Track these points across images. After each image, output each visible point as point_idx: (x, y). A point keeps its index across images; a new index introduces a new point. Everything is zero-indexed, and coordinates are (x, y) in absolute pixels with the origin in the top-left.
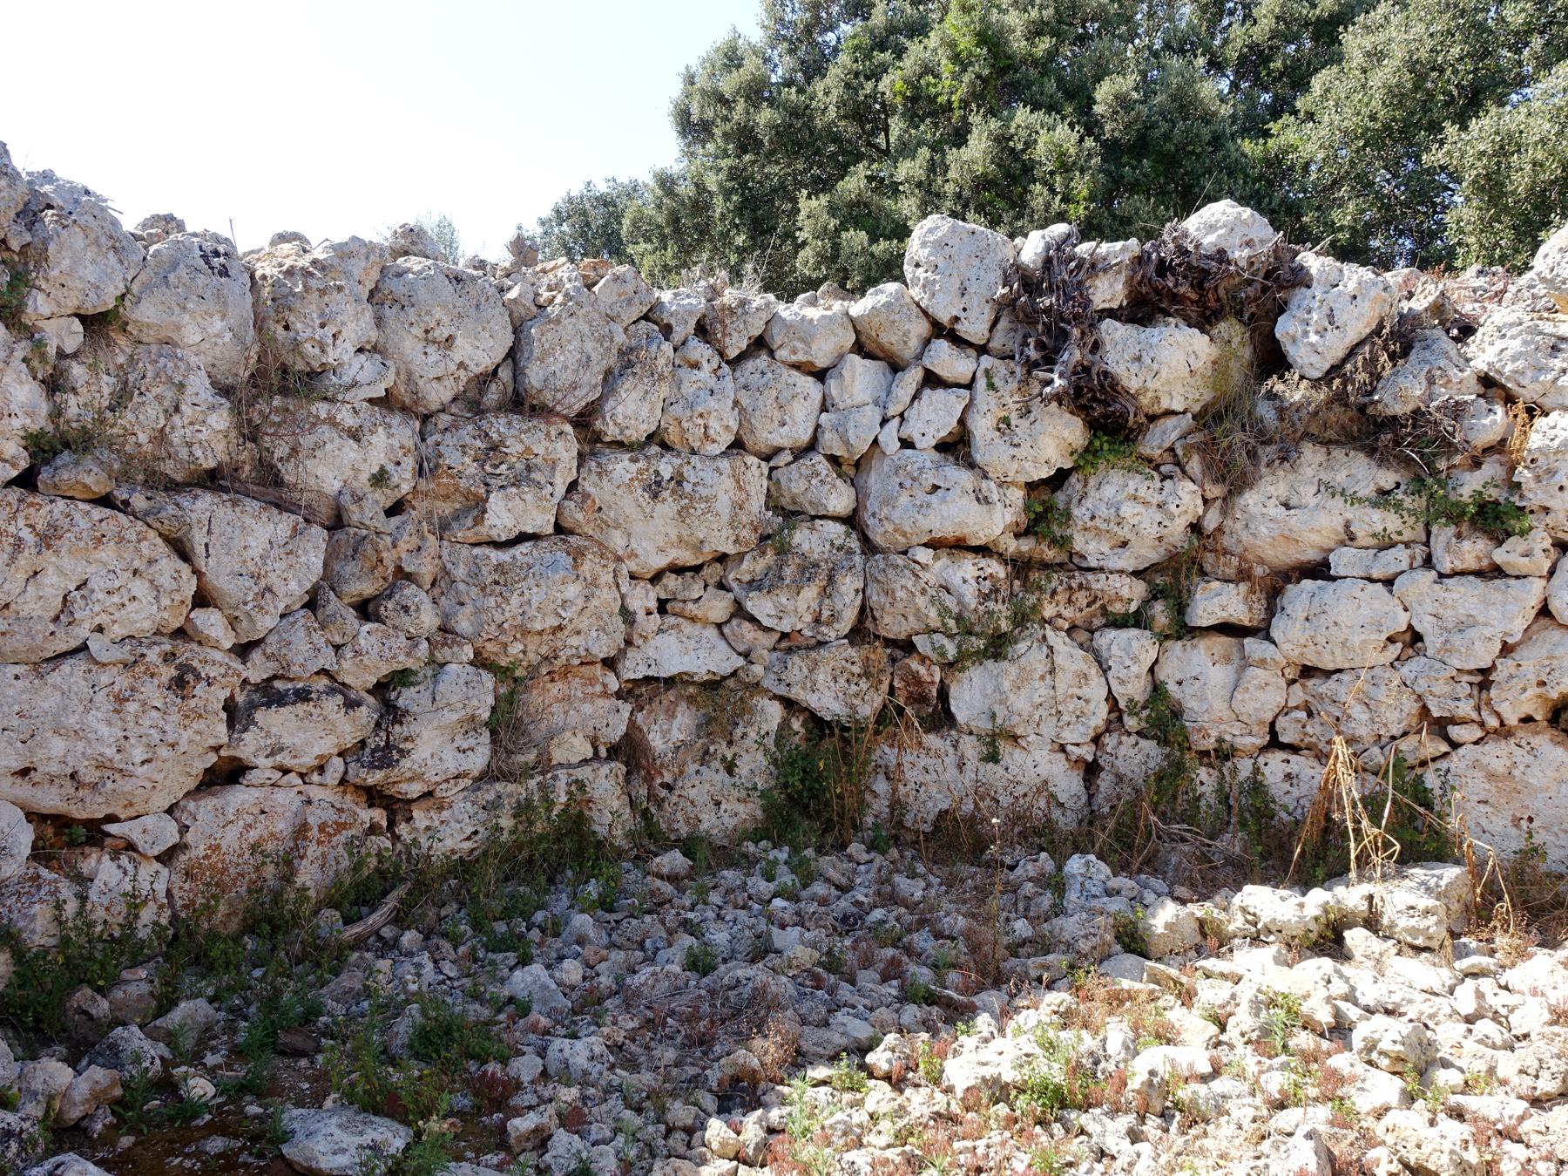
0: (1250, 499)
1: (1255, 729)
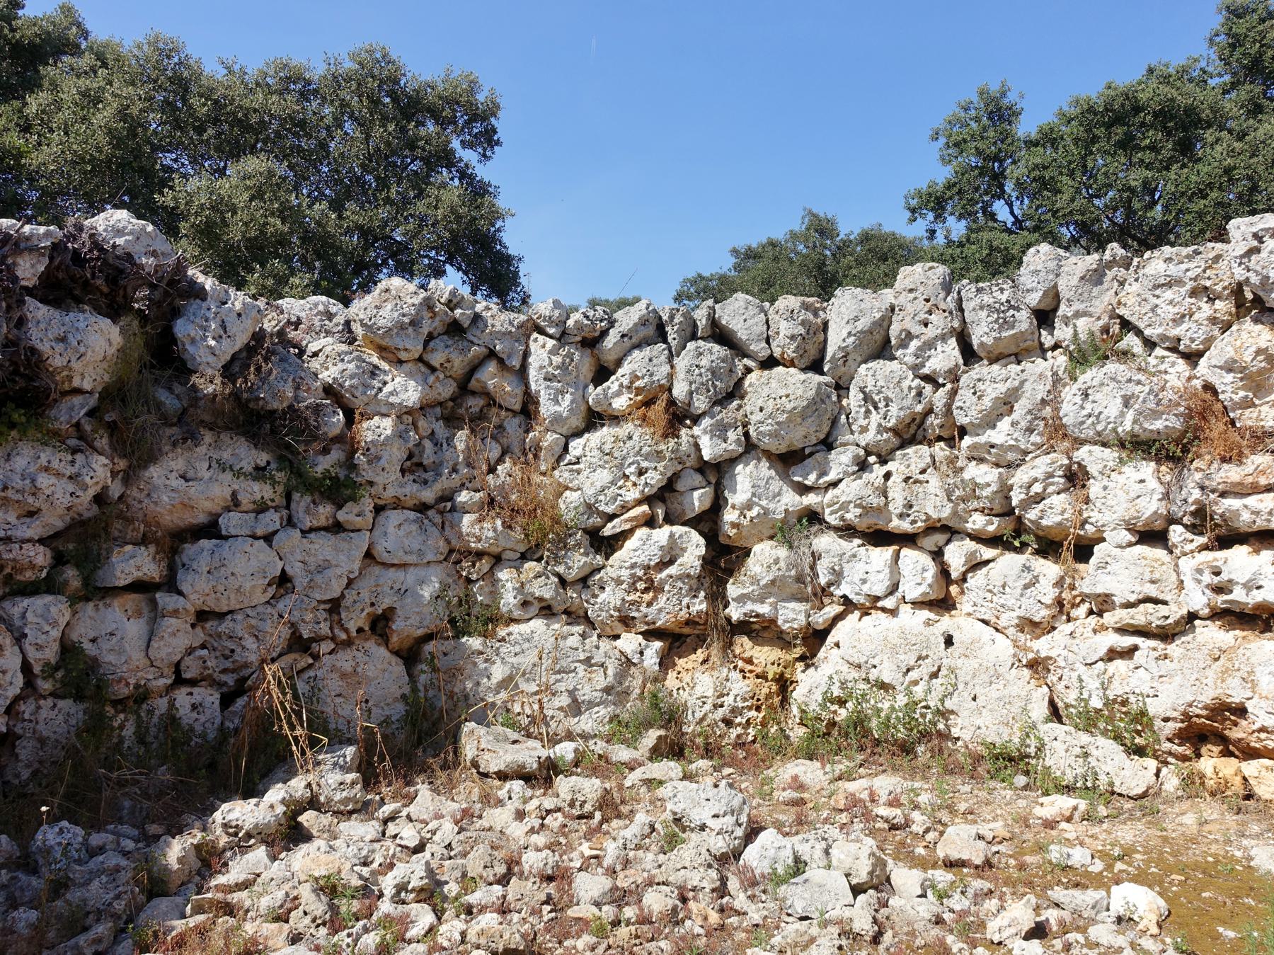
0: (155, 472)
1: (166, 671)
